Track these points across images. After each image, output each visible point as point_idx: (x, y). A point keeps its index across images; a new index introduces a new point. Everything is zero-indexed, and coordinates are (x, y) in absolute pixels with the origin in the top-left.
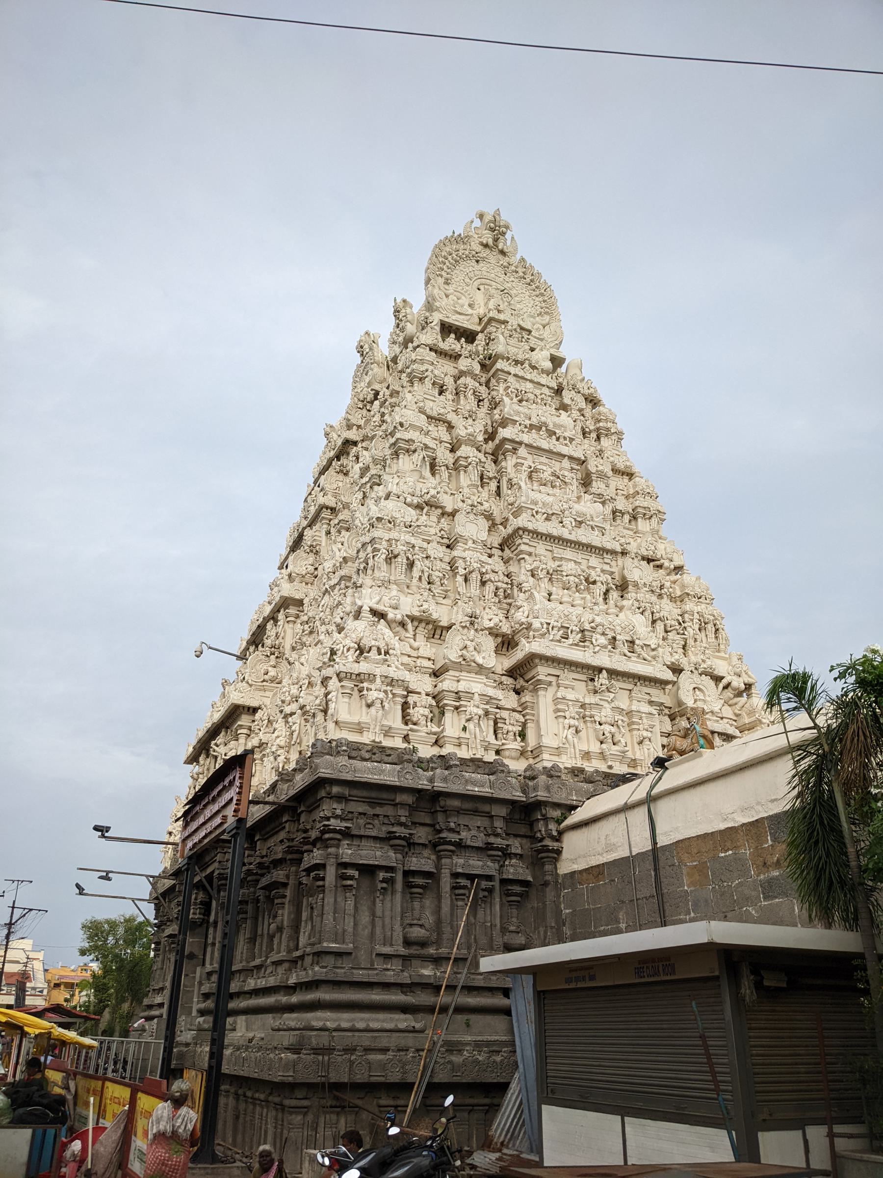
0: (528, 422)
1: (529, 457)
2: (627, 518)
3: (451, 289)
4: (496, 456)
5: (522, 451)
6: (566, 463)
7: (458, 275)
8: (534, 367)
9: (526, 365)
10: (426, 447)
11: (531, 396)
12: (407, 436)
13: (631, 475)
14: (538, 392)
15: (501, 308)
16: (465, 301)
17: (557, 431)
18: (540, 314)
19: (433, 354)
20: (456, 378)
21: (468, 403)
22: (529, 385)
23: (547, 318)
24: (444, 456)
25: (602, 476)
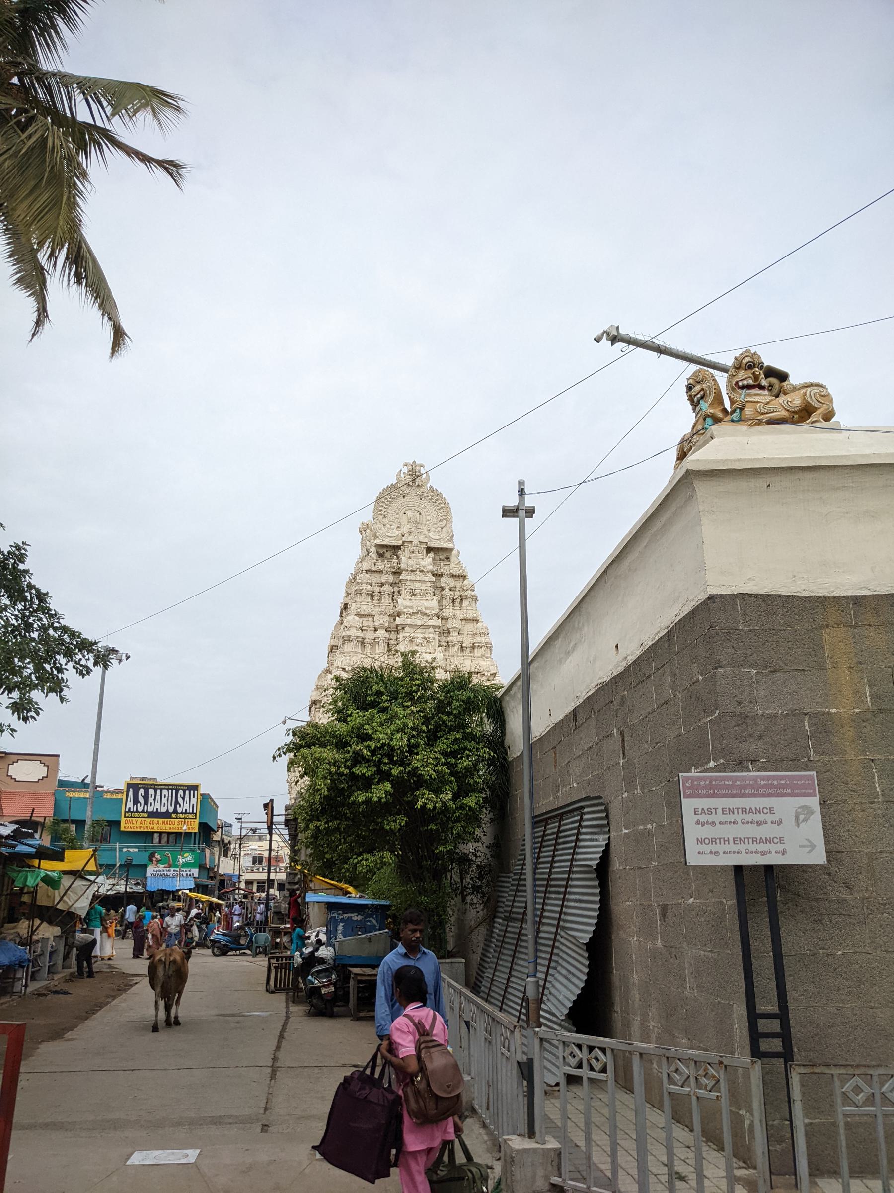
0: (411, 611)
1: (412, 630)
2: (468, 649)
3: (386, 521)
4: (397, 629)
5: (407, 629)
6: (431, 630)
7: (392, 509)
8: (422, 571)
9: (418, 572)
10: (357, 637)
11: (417, 591)
12: (348, 633)
13: (477, 621)
14: (423, 588)
15: (412, 530)
16: (394, 526)
17: (428, 612)
18: (441, 521)
19: (368, 576)
20: (382, 584)
21: (386, 599)
22: (418, 585)
23: (444, 522)
24: (369, 636)
25: (455, 629)
